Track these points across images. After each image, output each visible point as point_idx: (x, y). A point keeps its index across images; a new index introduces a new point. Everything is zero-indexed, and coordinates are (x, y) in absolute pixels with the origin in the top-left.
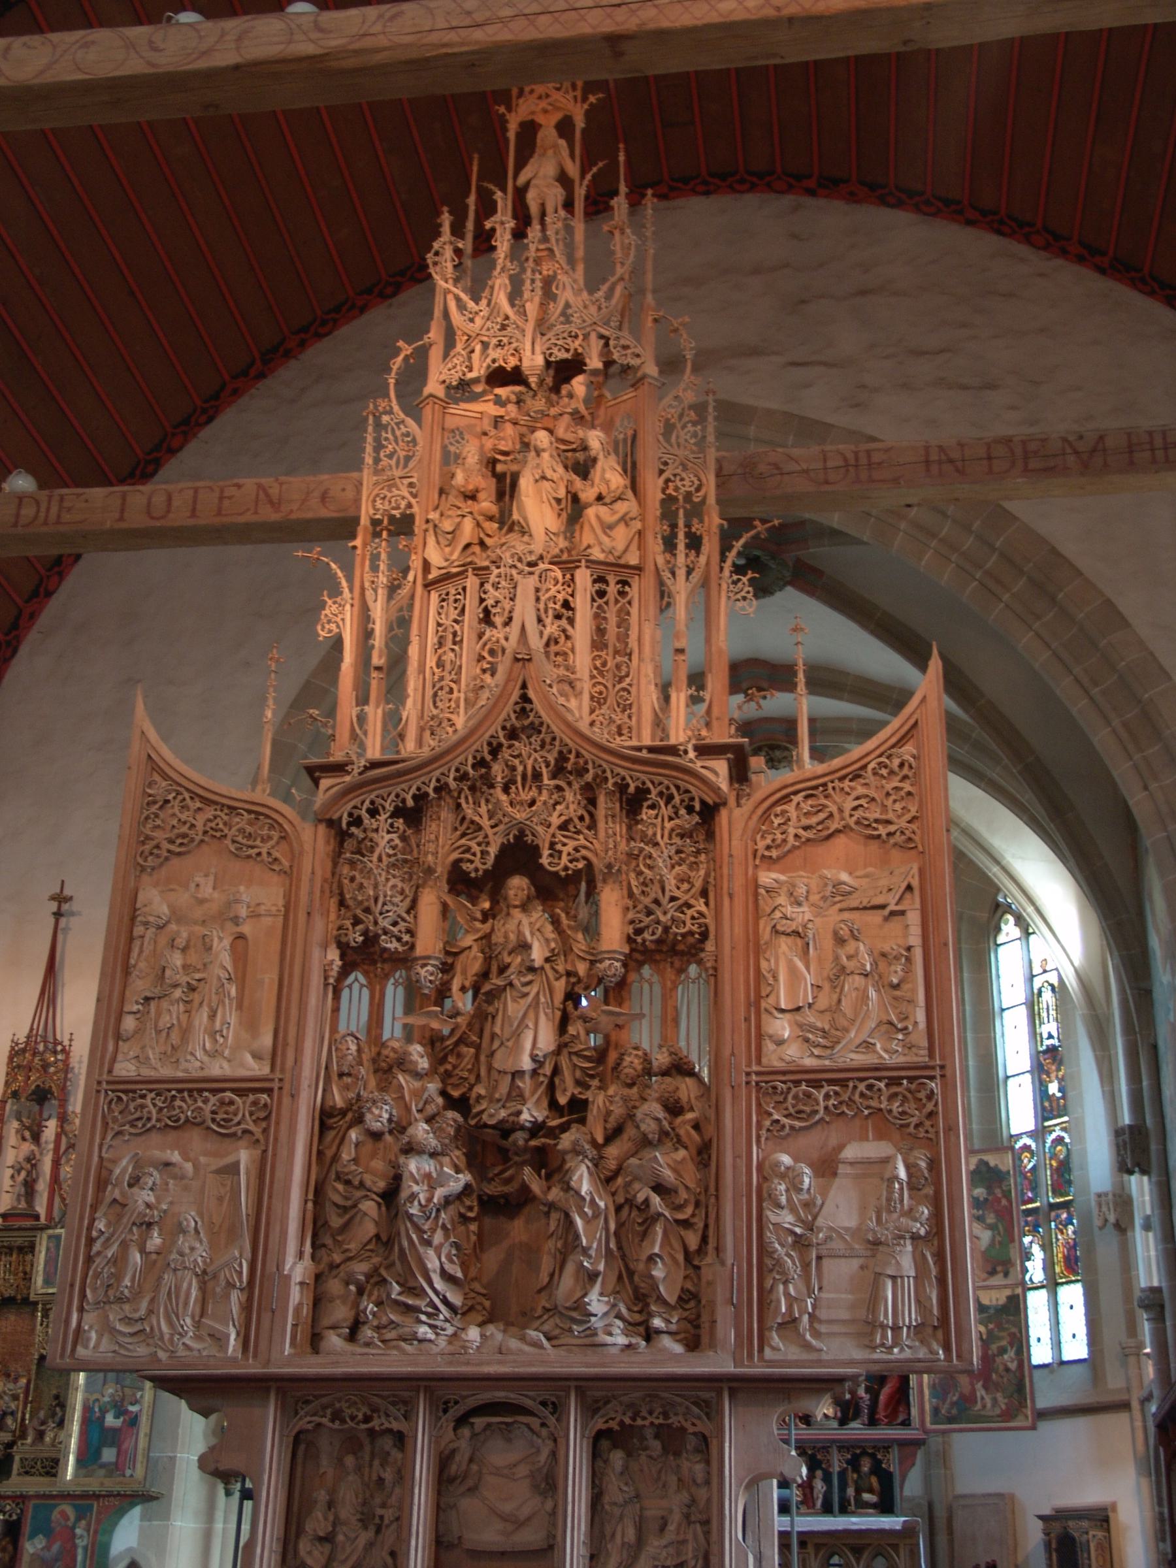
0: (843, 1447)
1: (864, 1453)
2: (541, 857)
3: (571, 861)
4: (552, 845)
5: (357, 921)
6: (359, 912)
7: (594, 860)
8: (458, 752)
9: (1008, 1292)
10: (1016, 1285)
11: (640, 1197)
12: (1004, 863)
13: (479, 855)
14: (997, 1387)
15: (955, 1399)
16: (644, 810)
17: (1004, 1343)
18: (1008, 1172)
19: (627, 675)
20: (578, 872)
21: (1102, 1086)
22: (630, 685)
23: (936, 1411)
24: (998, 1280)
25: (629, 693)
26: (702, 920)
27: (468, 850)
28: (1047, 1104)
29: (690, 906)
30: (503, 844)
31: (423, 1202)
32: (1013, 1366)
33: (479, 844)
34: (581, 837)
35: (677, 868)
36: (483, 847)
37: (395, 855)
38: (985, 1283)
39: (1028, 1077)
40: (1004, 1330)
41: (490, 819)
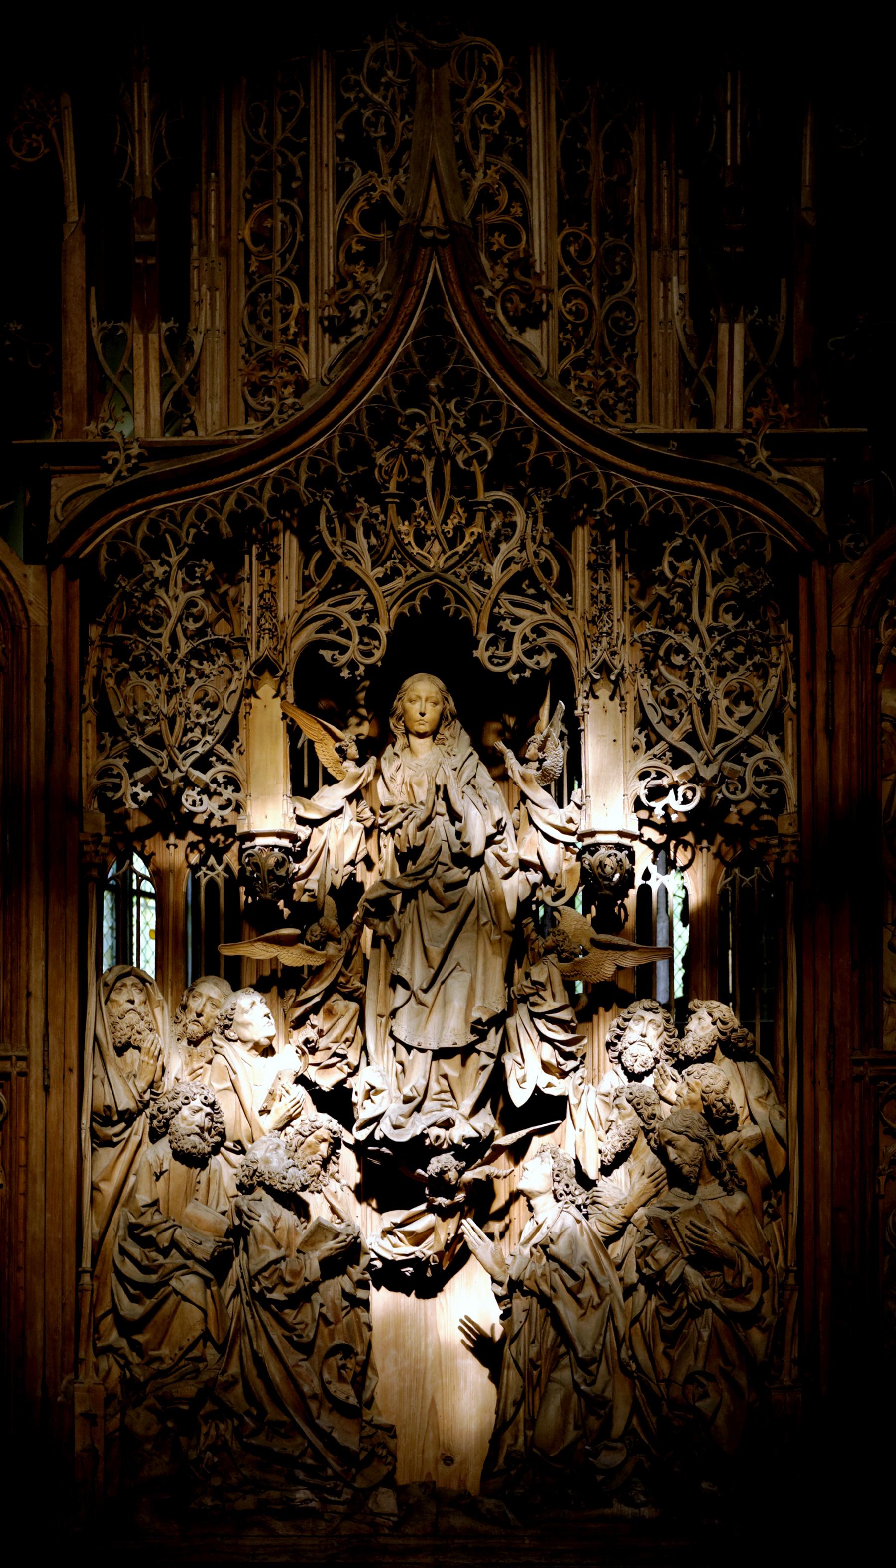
2: (477, 648)
3: (529, 653)
4: (494, 620)
5: (137, 761)
6: (138, 741)
7: (571, 651)
8: (314, 430)
11: (672, 1276)
13: (356, 638)
16: (666, 559)
19: (626, 274)
20: (538, 673)
22: (631, 295)
25: (631, 312)
26: (772, 777)
27: (335, 624)
29: (753, 750)
30: (401, 617)
31: (288, 1278)
33: (356, 615)
34: (546, 606)
35: (730, 676)
36: (364, 621)
37: (201, 633)
41: (374, 566)
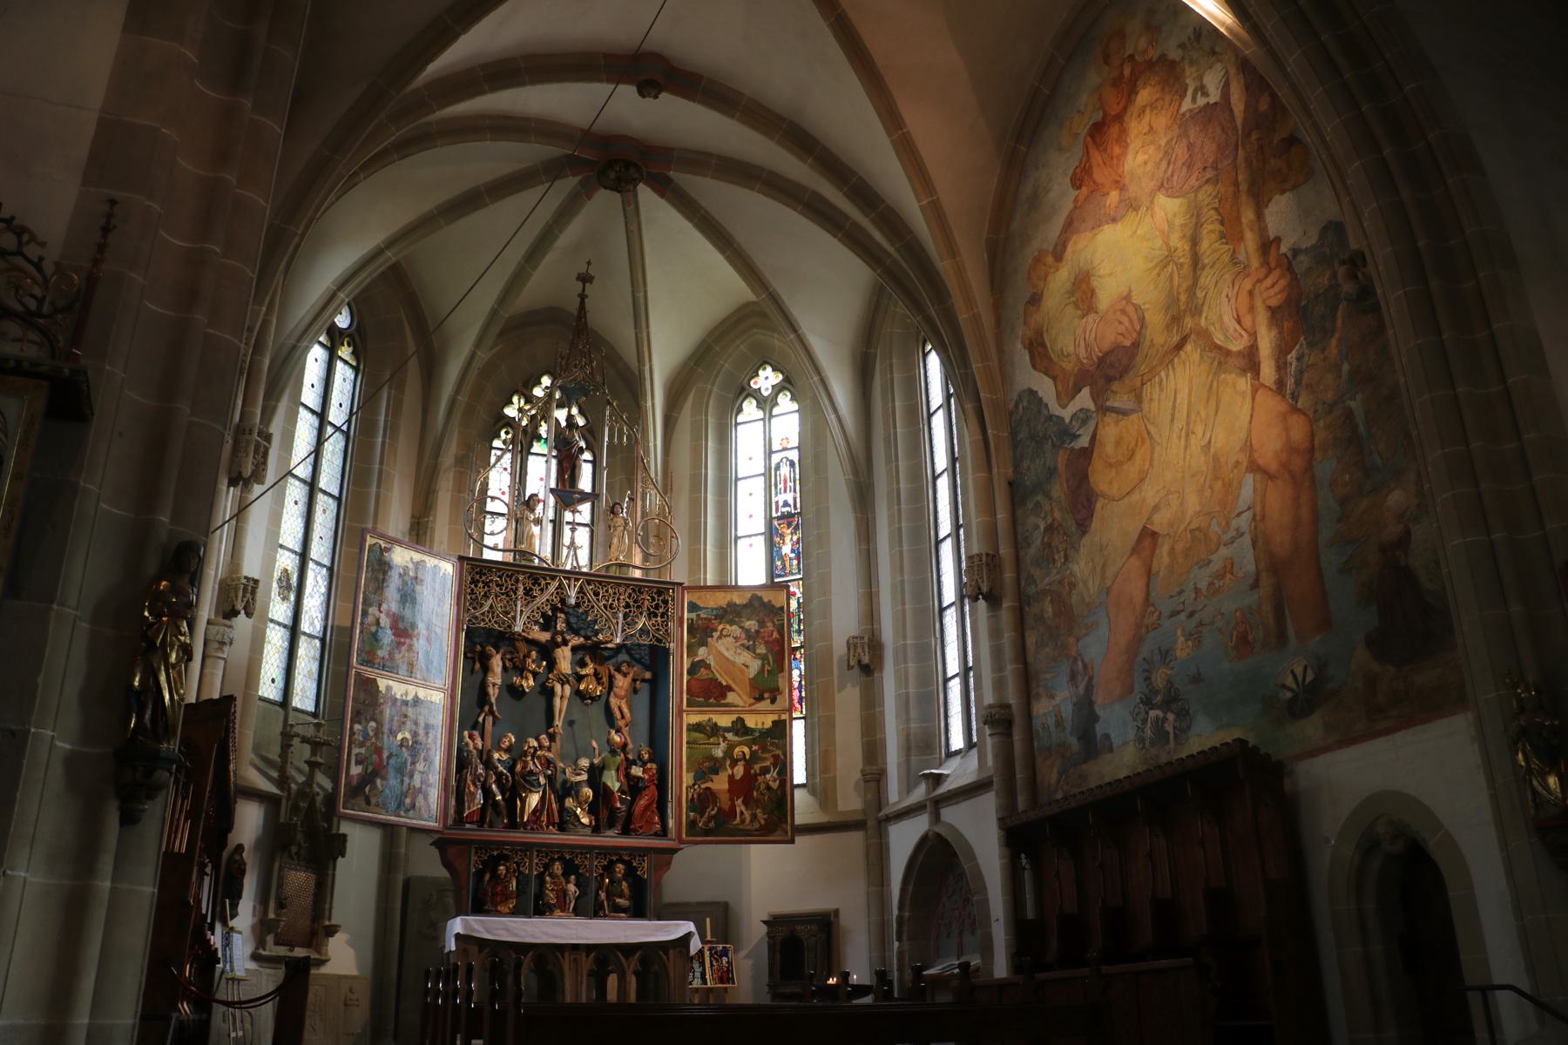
0: (600, 854)
1: (621, 861)
9: (775, 717)
10: (784, 711)
12: (800, 332)
14: (757, 803)
15: (713, 813)
17: (768, 763)
18: (783, 607)
21: (860, 545)
23: (692, 824)
24: (765, 705)
28: (779, 563)
32: (775, 785)
38: (753, 708)
39: (761, 539)
40: (769, 751)
